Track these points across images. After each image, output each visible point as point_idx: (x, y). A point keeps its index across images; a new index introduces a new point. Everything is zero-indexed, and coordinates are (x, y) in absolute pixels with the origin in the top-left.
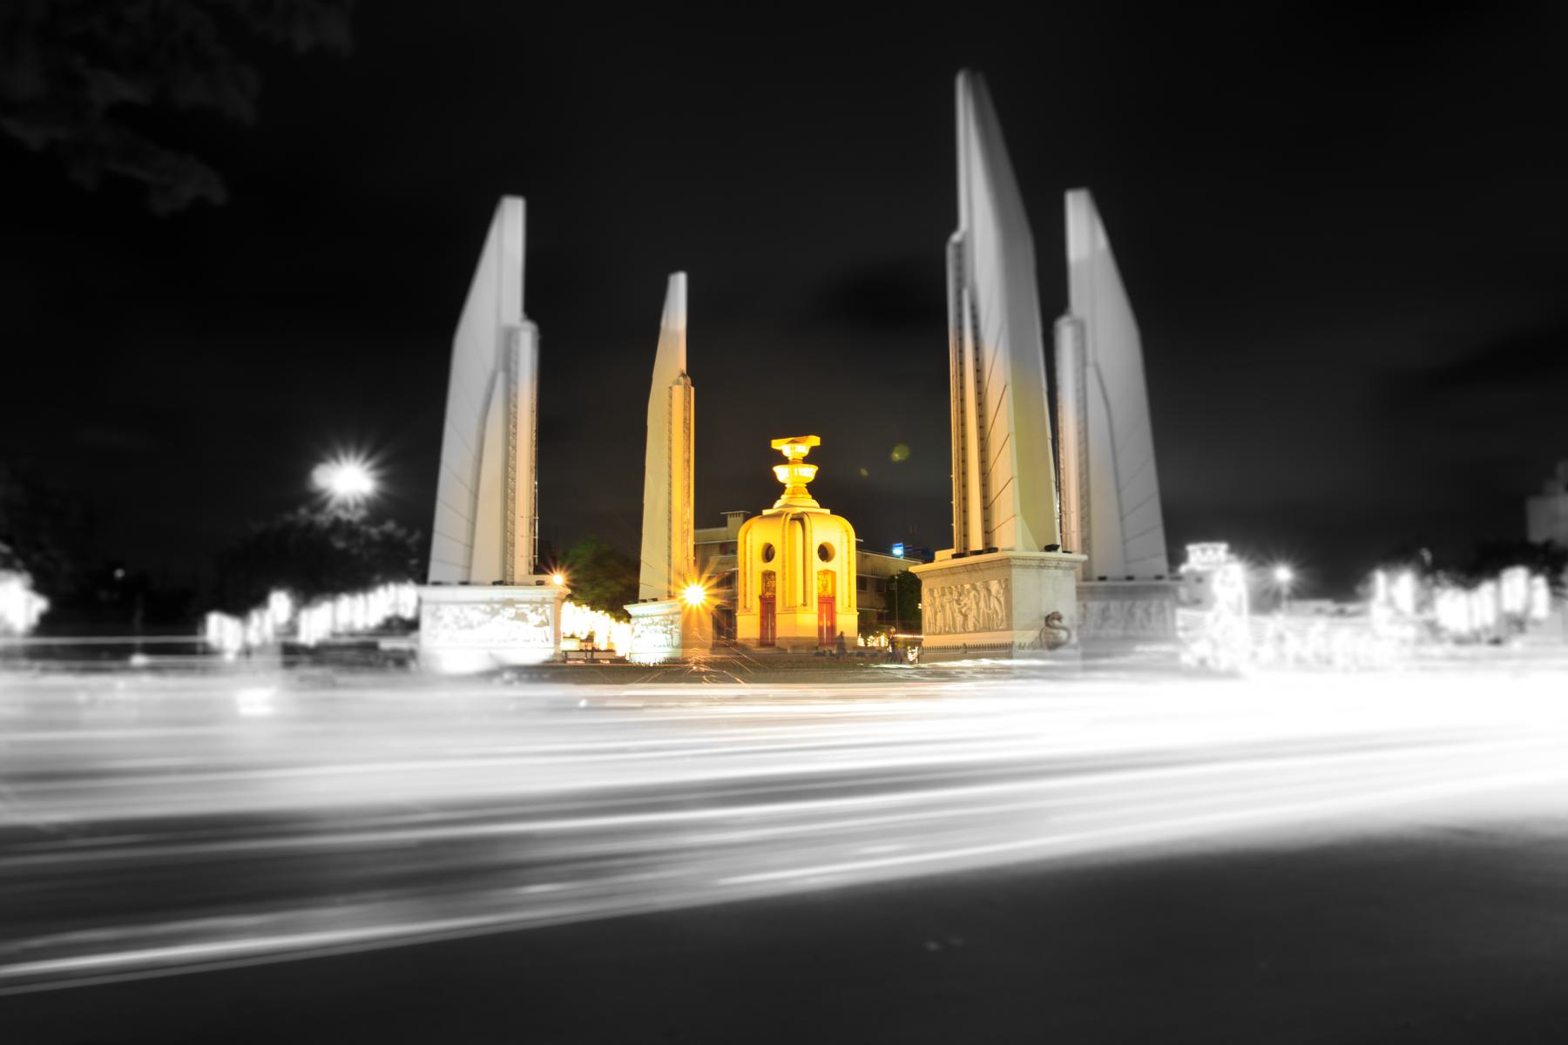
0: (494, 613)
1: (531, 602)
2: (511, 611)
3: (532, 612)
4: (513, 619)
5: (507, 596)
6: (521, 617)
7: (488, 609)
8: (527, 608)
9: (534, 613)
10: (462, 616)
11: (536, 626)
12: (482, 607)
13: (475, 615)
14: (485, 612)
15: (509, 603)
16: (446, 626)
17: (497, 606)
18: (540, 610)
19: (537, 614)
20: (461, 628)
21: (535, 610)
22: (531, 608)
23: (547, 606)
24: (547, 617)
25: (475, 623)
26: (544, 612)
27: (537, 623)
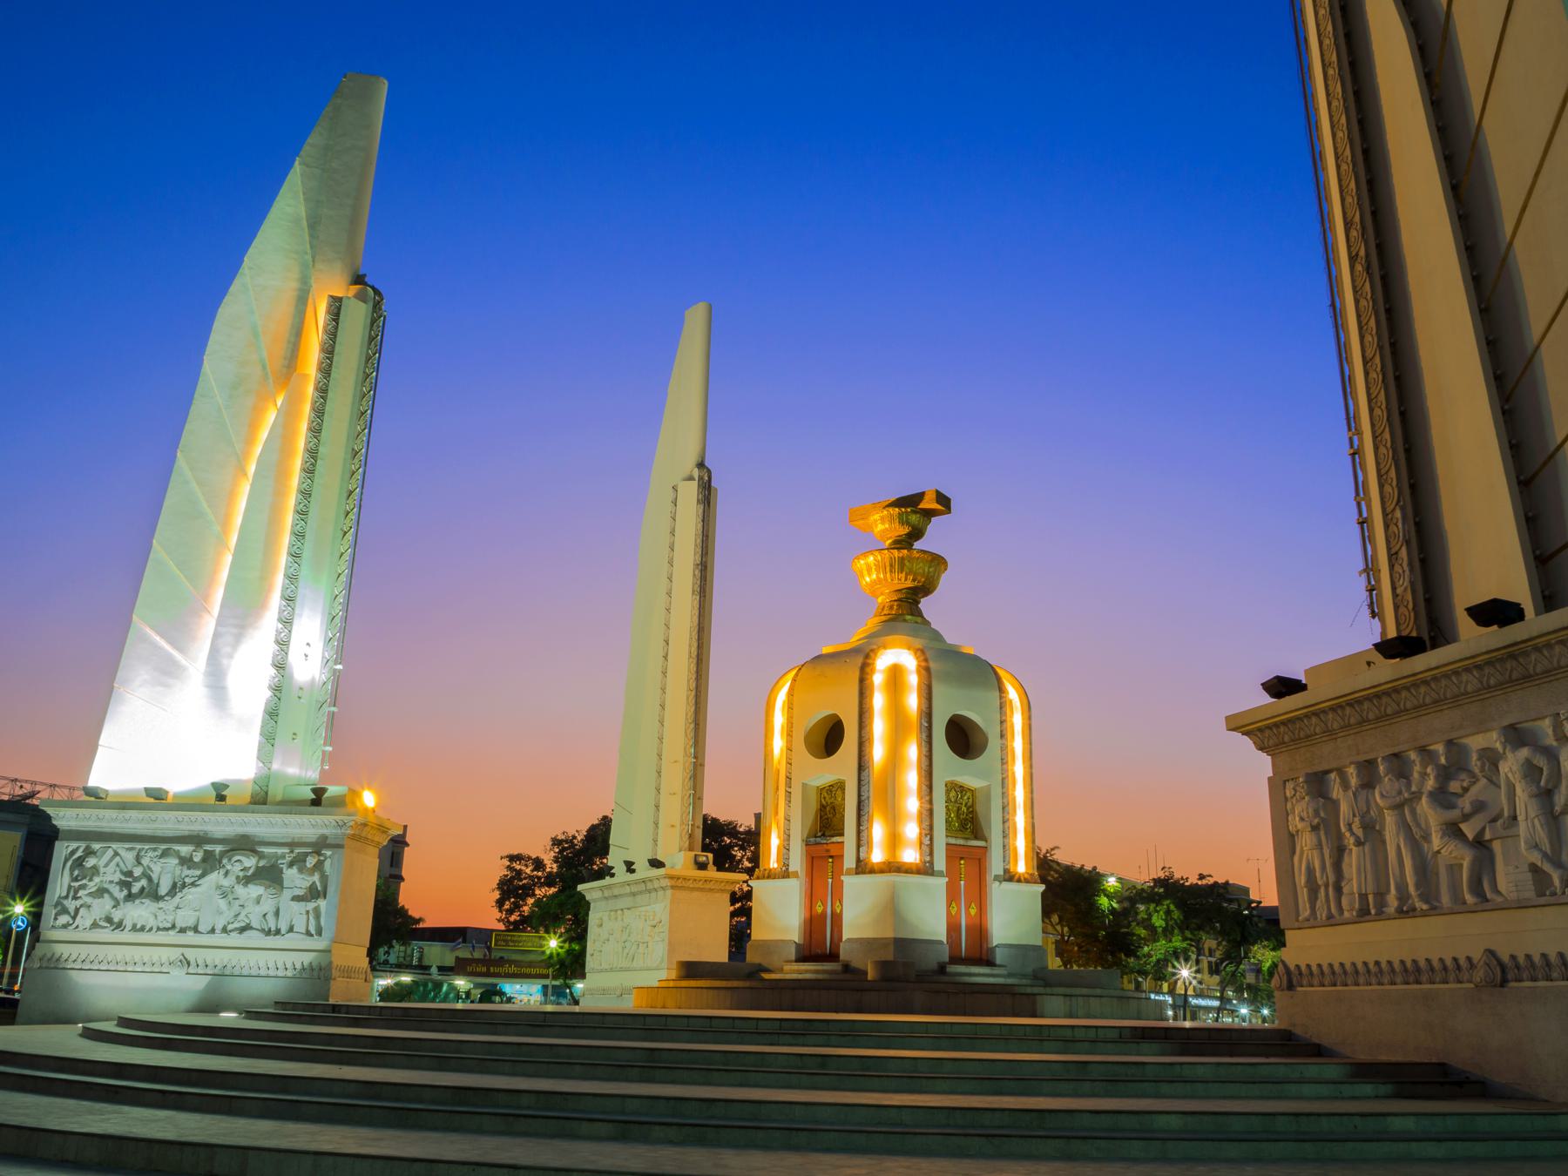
0: (211, 863)
1: (292, 845)
2: (250, 862)
3: (291, 865)
4: (247, 880)
5: (241, 830)
6: (269, 875)
7: (198, 857)
8: (283, 857)
9: (294, 870)
10: (137, 872)
11: (296, 898)
12: (185, 850)
13: (165, 871)
14: (186, 862)
15: (244, 844)
16: (101, 892)
17: (218, 849)
18: (311, 861)
19: (301, 871)
20: (130, 897)
21: (298, 862)
22: (288, 859)
23: (329, 853)
24: (324, 879)
25: (163, 891)
26: (319, 866)
27: (301, 892)
